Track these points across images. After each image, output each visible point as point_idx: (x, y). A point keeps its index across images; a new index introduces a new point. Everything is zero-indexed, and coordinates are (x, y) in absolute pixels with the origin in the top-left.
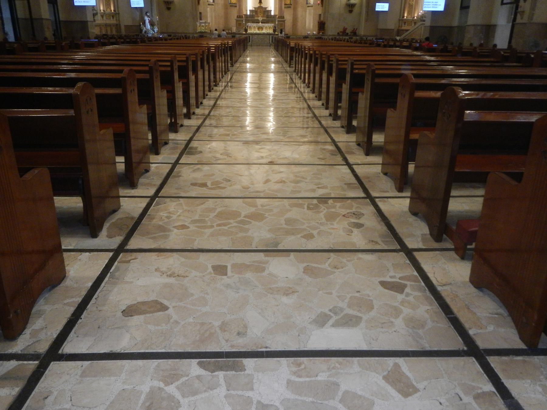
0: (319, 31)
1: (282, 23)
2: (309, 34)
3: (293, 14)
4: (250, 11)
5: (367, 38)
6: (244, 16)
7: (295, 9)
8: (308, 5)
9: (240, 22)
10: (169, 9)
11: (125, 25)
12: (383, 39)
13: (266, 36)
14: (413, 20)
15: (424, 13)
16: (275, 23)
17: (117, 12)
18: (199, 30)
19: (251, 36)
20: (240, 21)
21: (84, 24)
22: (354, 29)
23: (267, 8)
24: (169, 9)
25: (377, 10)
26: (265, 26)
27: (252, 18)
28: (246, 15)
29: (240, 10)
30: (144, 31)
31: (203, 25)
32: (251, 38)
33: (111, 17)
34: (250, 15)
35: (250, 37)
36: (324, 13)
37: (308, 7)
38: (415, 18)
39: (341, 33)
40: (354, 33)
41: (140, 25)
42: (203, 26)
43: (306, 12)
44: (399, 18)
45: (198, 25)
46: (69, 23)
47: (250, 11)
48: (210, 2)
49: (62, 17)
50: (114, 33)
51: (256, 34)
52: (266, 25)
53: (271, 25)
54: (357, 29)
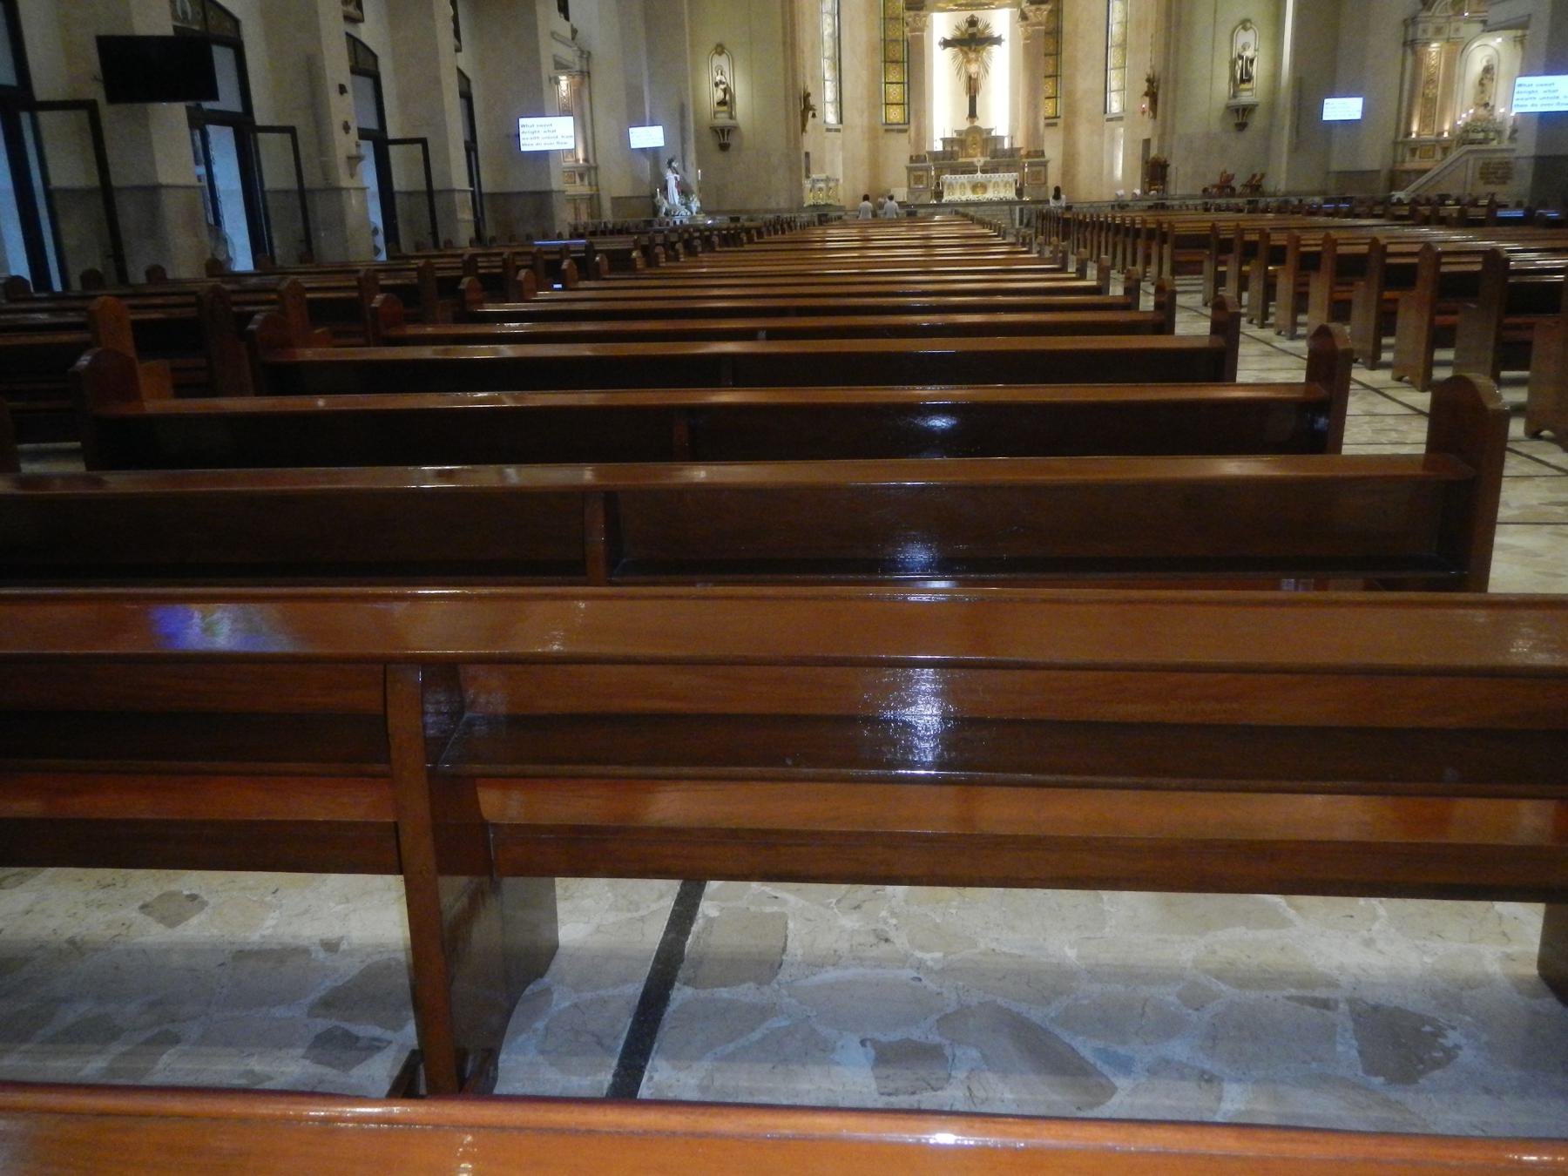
0: (1150, 186)
1: (1034, 169)
2: (1122, 196)
3: (1065, 144)
4: (945, 141)
5: (1300, 201)
7: (1069, 129)
9: (920, 173)
10: (724, 147)
11: (616, 195)
12: (1345, 200)
13: (999, 207)
14: (1437, 141)
15: (1473, 121)
17: (591, 161)
18: (809, 200)
20: (916, 169)
21: (542, 200)
22: (1254, 176)
23: (992, 129)
24: (724, 147)
25: (1325, 118)
27: (952, 158)
28: (935, 156)
29: (921, 137)
30: (664, 210)
33: (578, 180)
36: (1162, 137)
37: (1108, 120)
38: (1446, 135)
39: (1215, 190)
40: (1255, 187)
41: (654, 196)
42: (821, 189)
43: (1101, 135)
44: (1391, 134)
45: (807, 184)
46: (503, 199)
47: (945, 141)
48: (828, 124)
49: (487, 186)
50: (584, 218)
53: (1011, 177)
54: (1263, 176)
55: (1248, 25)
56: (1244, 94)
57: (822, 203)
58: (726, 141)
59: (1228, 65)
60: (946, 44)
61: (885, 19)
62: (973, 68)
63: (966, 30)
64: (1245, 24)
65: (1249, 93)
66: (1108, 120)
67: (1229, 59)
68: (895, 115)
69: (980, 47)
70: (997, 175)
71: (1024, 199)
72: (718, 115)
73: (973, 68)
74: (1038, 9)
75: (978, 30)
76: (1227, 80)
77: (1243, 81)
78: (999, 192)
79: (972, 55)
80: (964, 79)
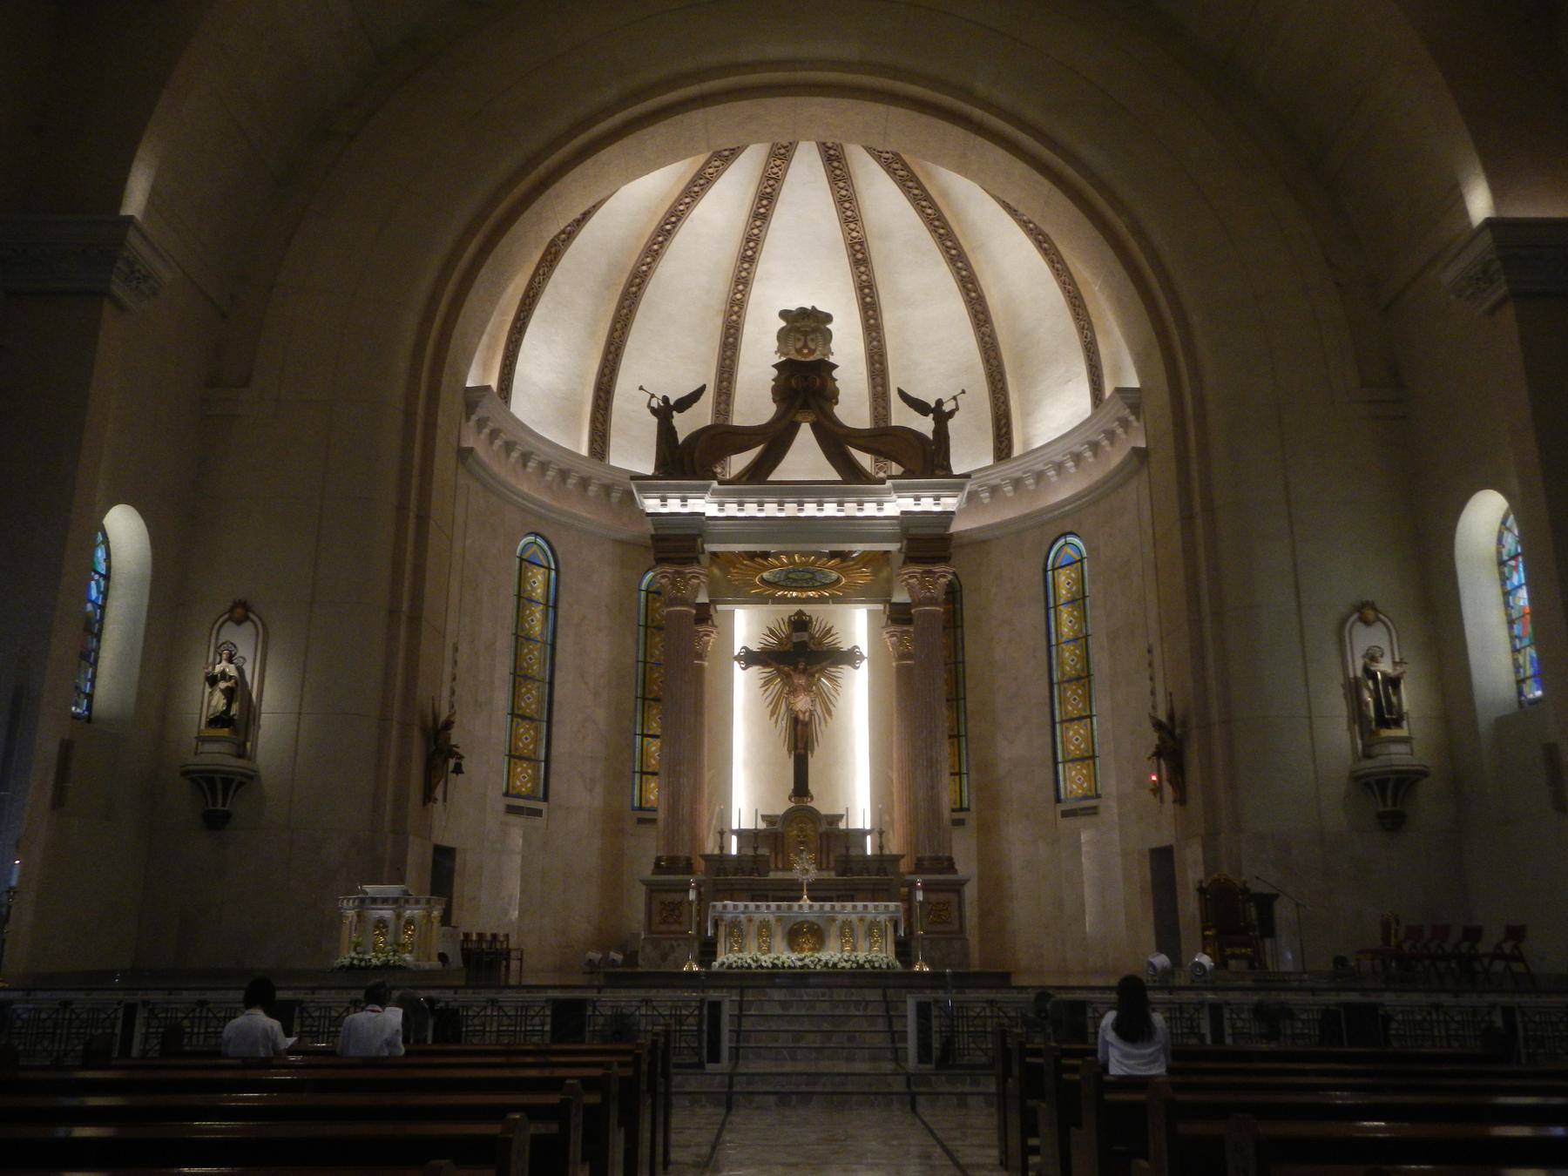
1: (942, 897)
6: (700, 865)
7: (988, 831)
8: (1062, 807)
9: (676, 897)
16: (909, 900)
18: (346, 957)
19: (728, 1001)
23: (841, 817)
24: (215, 821)
26: (840, 917)
28: (720, 862)
31: (387, 913)
32: (727, 1011)
34: (740, 856)
35: (716, 1007)
37: (1065, 814)
42: (381, 924)
47: (741, 834)
51: (775, 976)
52: (847, 910)
53: (881, 911)
55: (1370, 614)
56: (1394, 748)
57: (374, 961)
58: (219, 807)
59: (1341, 691)
60: (750, 658)
61: (646, 626)
62: (802, 703)
63: (788, 637)
64: (1365, 612)
65: (1402, 748)
66: (1065, 814)
67: (1340, 679)
68: (653, 792)
69: (818, 667)
70: (849, 905)
71: (917, 968)
72: (207, 747)
73: (802, 703)
74: (929, 573)
75: (812, 637)
76: (1343, 722)
77: (1383, 722)
78: (854, 949)
79: (800, 681)
80: (783, 723)
